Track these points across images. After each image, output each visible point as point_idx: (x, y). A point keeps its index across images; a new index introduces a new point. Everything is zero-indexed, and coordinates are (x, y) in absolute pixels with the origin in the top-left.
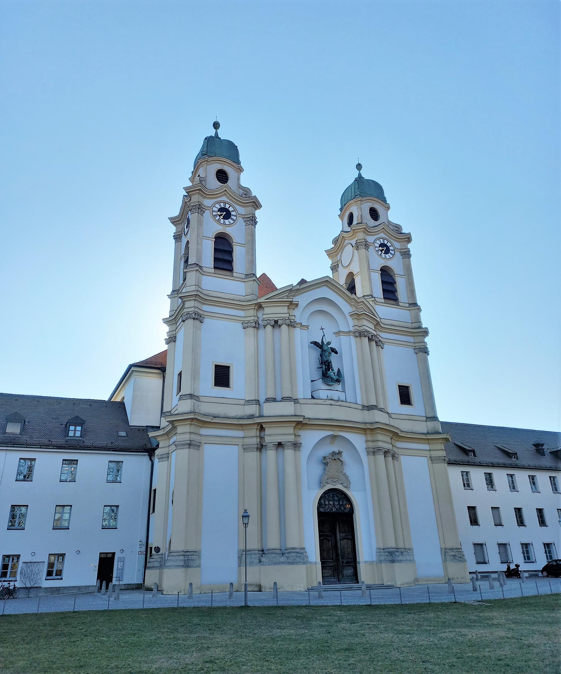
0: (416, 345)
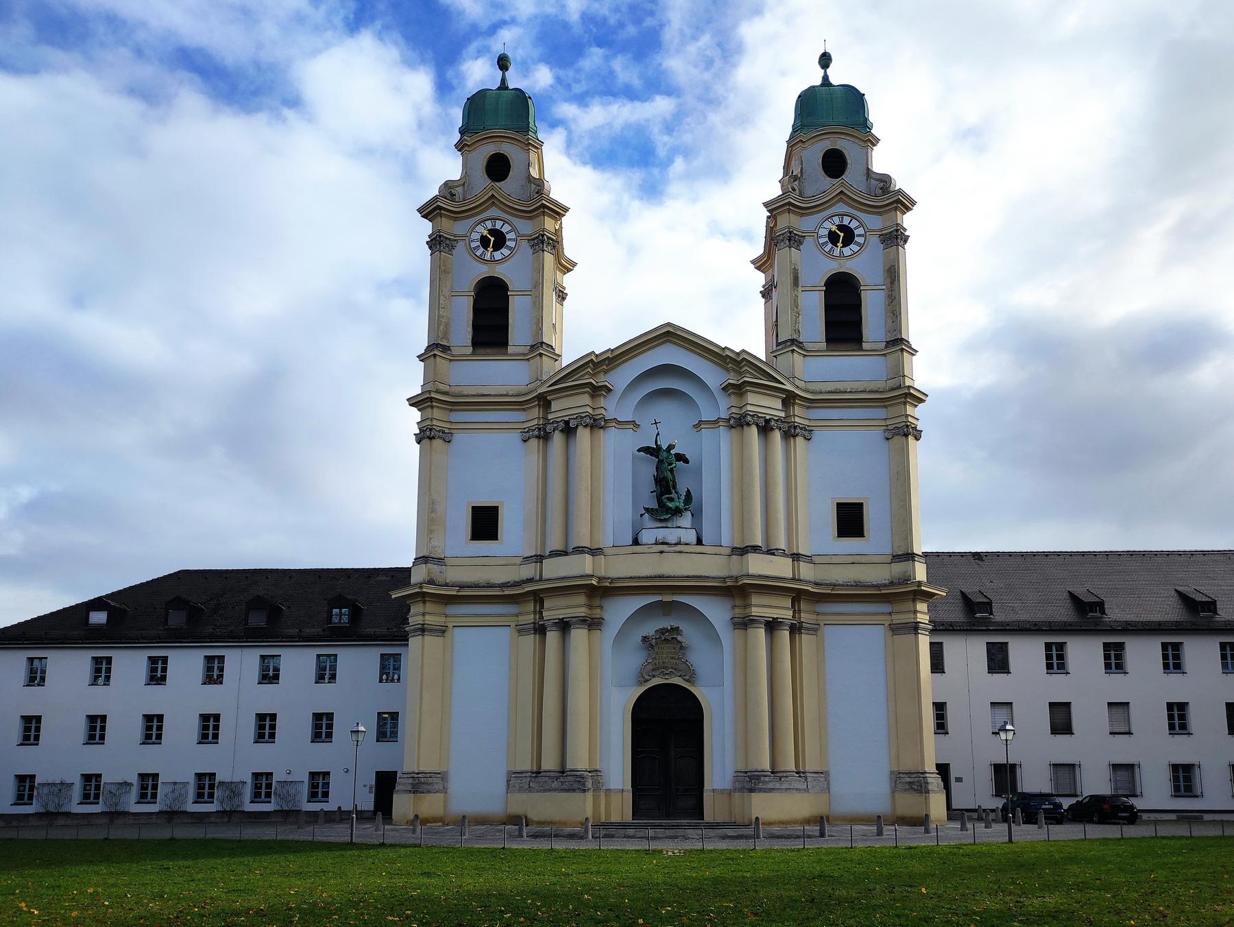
0: (888, 422)
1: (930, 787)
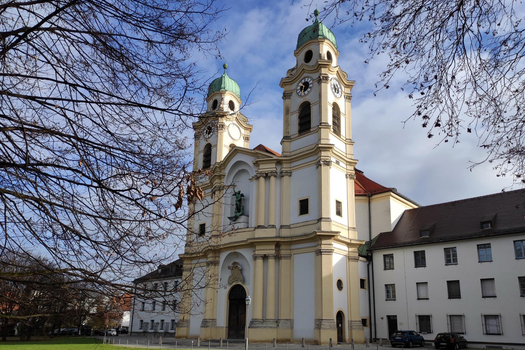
1: (322, 326)
